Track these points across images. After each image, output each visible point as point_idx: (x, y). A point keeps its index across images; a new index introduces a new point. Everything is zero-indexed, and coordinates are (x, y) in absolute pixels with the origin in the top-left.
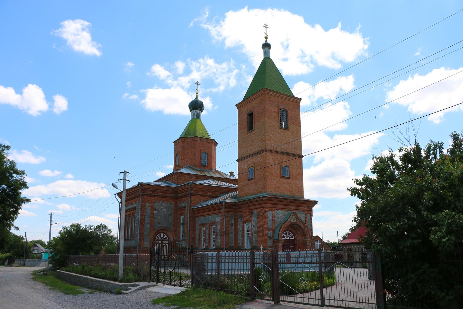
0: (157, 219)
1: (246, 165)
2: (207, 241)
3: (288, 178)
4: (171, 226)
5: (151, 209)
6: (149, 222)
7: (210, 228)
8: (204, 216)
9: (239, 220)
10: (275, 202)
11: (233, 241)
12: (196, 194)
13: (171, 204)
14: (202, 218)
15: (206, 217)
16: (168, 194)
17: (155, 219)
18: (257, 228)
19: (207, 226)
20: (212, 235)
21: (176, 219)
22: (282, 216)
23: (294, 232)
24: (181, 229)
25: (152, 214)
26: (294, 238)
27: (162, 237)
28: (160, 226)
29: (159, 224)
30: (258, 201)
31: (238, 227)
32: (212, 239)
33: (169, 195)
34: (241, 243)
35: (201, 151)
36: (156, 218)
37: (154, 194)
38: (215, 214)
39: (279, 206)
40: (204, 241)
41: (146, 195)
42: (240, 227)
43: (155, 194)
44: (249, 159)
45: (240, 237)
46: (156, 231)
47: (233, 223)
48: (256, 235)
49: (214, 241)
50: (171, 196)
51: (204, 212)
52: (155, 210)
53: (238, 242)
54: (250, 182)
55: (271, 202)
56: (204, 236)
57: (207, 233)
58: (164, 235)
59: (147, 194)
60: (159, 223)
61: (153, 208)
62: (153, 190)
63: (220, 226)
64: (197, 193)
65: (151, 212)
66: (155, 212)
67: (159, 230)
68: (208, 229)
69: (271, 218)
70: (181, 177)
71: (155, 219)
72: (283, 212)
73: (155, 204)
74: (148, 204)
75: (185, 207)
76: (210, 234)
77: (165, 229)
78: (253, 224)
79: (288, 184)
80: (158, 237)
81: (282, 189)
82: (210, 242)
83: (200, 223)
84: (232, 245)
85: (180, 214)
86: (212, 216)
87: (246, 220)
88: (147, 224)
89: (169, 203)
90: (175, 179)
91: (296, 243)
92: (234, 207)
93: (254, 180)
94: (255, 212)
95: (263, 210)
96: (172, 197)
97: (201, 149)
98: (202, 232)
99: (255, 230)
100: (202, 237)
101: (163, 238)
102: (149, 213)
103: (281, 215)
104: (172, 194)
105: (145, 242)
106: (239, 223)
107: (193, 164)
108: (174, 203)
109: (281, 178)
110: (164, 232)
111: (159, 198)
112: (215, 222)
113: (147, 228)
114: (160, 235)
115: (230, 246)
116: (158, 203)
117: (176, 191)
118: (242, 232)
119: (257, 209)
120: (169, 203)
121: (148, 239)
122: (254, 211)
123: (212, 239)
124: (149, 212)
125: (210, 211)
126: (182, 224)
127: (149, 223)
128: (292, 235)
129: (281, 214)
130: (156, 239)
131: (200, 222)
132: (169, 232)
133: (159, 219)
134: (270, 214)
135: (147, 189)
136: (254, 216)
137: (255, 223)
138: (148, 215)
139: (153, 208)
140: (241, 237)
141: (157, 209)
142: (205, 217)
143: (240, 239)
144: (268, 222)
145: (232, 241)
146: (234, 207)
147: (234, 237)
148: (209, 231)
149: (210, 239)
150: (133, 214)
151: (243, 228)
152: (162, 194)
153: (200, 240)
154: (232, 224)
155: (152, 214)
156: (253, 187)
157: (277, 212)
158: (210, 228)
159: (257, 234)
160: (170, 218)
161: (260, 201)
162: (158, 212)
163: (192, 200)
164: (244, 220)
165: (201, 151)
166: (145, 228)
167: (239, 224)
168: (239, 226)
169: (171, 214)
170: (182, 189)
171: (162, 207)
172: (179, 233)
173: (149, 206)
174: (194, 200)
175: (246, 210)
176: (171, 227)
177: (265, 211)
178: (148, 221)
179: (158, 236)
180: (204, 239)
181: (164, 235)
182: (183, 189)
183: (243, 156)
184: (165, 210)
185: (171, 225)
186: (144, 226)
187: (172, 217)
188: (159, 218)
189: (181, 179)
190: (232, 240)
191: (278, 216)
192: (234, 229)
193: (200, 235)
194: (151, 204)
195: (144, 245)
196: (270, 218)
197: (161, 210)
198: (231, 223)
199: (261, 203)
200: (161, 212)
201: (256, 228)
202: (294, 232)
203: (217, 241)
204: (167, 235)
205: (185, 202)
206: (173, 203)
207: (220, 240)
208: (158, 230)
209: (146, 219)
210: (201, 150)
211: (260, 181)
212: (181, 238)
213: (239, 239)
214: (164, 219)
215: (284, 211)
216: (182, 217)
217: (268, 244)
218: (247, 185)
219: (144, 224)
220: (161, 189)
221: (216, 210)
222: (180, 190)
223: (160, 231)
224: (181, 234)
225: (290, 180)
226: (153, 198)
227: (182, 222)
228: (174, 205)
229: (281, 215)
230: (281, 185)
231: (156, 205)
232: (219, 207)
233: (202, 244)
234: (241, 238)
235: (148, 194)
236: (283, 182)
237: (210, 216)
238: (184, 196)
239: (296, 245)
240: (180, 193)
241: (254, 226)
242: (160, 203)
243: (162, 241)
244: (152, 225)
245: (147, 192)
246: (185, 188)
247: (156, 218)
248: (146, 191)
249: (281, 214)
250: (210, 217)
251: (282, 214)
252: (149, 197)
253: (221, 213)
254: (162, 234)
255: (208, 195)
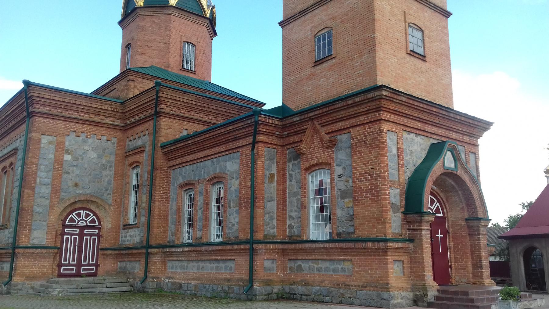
0: (71, 174)
1: (309, 27)
2: (199, 224)
3: (423, 58)
4: (108, 192)
5: (56, 151)
6: (48, 181)
7: (207, 192)
8: (192, 163)
9: (291, 166)
10: (405, 108)
11: (275, 222)
12: (172, 115)
13: (109, 142)
14: (188, 167)
15: (199, 164)
16: (103, 117)
17: (65, 176)
18: (350, 181)
19: (200, 187)
20: (213, 207)
21: (121, 176)
22: (419, 149)
23: (442, 199)
24: (133, 199)
25: (58, 162)
26: (441, 215)
27: (83, 220)
28: (79, 191)
29: (75, 188)
30: (356, 106)
31: (288, 182)
32: (213, 218)
33: (103, 120)
34: (298, 227)
35: (181, 38)
36: (69, 173)
37: (65, 113)
38: (224, 154)
39: (412, 123)
40: (189, 226)
41: (42, 116)
42: (294, 182)
43: (69, 116)
44: (316, 11)
45: (292, 210)
46: (68, 203)
47: (273, 174)
48: (346, 200)
49: (220, 223)
50: (110, 122)
51: (194, 152)
52: (67, 152)
53: (288, 222)
54: (319, 67)
55: (396, 109)
56: (190, 213)
57: (199, 203)
58: (87, 215)
59: (47, 111)
60: (76, 185)
61: (60, 148)
62: (64, 104)
63: (237, 182)
64: (174, 112)
65: (55, 156)
66: (67, 157)
67: (75, 203)
68: (204, 193)
69: (395, 151)
70: (136, 84)
71: (65, 176)
72: (422, 141)
73: (68, 138)
74: (50, 138)
75: (143, 147)
76: (207, 204)
77: (93, 200)
78: (338, 170)
79: (422, 72)
80: (72, 220)
81: (411, 83)
82: (206, 227)
83: (181, 181)
84: (272, 231)
85: (130, 165)
86: (215, 160)
87: (314, 162)
88: (44, 187)
89: (105, 138)
90: (122, 88)
91: (448, 227)
92: (277, 133)
93: (335, 61)
94: (343, 138)
95: (374, 128)
96: (111, 124)
97: (182, 34)
98: (187, 202)
99: (343, 188)
100: (186, 215)
101: (86, 221)
102: (51, 159)
103: (415, 147)
104: (111, 119)
105: (35, 232)
106: (291, 172)
107: (164, 64)
108: (116, 139)
109: (407, 53)
110: (89, 207)
111: (79, 126)
112: (224, 173)
113: (41, 195)
114: (79, 215)
115: (266, 233)
116: (76, 136)
117: (121, 111)
118: (299, 197)
119: (351, 130)
120: (105, 138)
121: (44, 223)
122: (339, 137)
123: (213, 218)
124: (52, 156)
125: (210, 148)
126: (136, 187)
127: (49, 184)
128: (438, 206)
129: (416, 144)
130: (67, 223)
131: (180, 178)
132: (101, 207)
133: (78, 175)
134: (392, 141)
135: (45, 100)
136: (340, 149)
137: (344, 168)
138: (47, 163)
139: (60, 148)
140: (296, 211)
141: (72, 151)
142: (195, 165)
143: (294, 214)
144: (389, 164)
145: (272, 219)
146: (277, 133)
147: (276, 211)
148: (206, 198)
149: (206, 218)
150: (11, 164)
151: (303, 187)
152: (87, 117)
153: (178, 223)
154: (272, 176)
155: (58, 162)
156: (332, 79)
157: (408, 139)
158: (207, 190)
159: (351, 199)
160: (104, 173)
161: (365, 106)
162: (75, 159)
163: (164, 127)
164: (307, 165)
165: (181, 38)
166: (36, 195)
167: (291, 176)
168: (291, 181)
169: (108, 165)
170: (137, 105)
171: (86, 148)
172: (126, 210)
173: (50, 143)
174: (166, 128)
175: (312, 136)
176: (108, 194)
177: (380, 132)
178: (46, 178)
179: (74, 216)
180: (190, 220)
181: (87, 215)
182: (140, 104)
183: (300, 8)
184: (93, 155)
185: (107, 190)
186: (34, 192)
187: (111, 171)
188: (78, 172)
189: (135, 87)
190: (272, 218)
191: (411, 148)
192: (277, 190)
193: (179, 211)
194: (55, 138)
195: (31, 238)
196: (391, 152)
197: (84, 153)
198: (268, 173)
199: (366, 109)
200: (83, 158)
201: (347, 181)
202: (442, 199)
203: (228, 222)
204: (95, 214)
205: (145, 135)
206: (115, 140)
207: (237, 220)
208: (72, 201)
209: (41, 174)
210: (181, 36)
211: (352, 60)
212: (131, 222)
213: (291, 217)
214: (90, 175)
215: (422, 137)
216: (135, 172)
217: (392, 224)
218: (310, 77)
219: (33, 185)
220: (85, 104)
221: (228, 141)
222: (131, 108)
223: (78, 205)
224: (132, 211)
225: (427, 64)
226: (61, 125)
227: (134, 183)
228: (115, 145)
229: (418, 147)
230: (409, 74)
231: (70, 141)
232: (236, 133)
233: (186, 234)
234: (297, 213)
235: (50, 112)
236: (411, 65)
237: (210, 161)
238: (143, 119)
239: (449, 233)
240: (133, 117)
241: (340, 176)
242: (81, 138)
243: (82, 228)
244: (55, 189)
245: (48, 108)
246: (145, 101)
247: (69, 173)
248: (44, 105)
249: (417, 145)
250: (208, 163)
251: (419, 144)
252: (50, 120)
253: (239, 150)
254: (83, 213)
255: (200, 121)
